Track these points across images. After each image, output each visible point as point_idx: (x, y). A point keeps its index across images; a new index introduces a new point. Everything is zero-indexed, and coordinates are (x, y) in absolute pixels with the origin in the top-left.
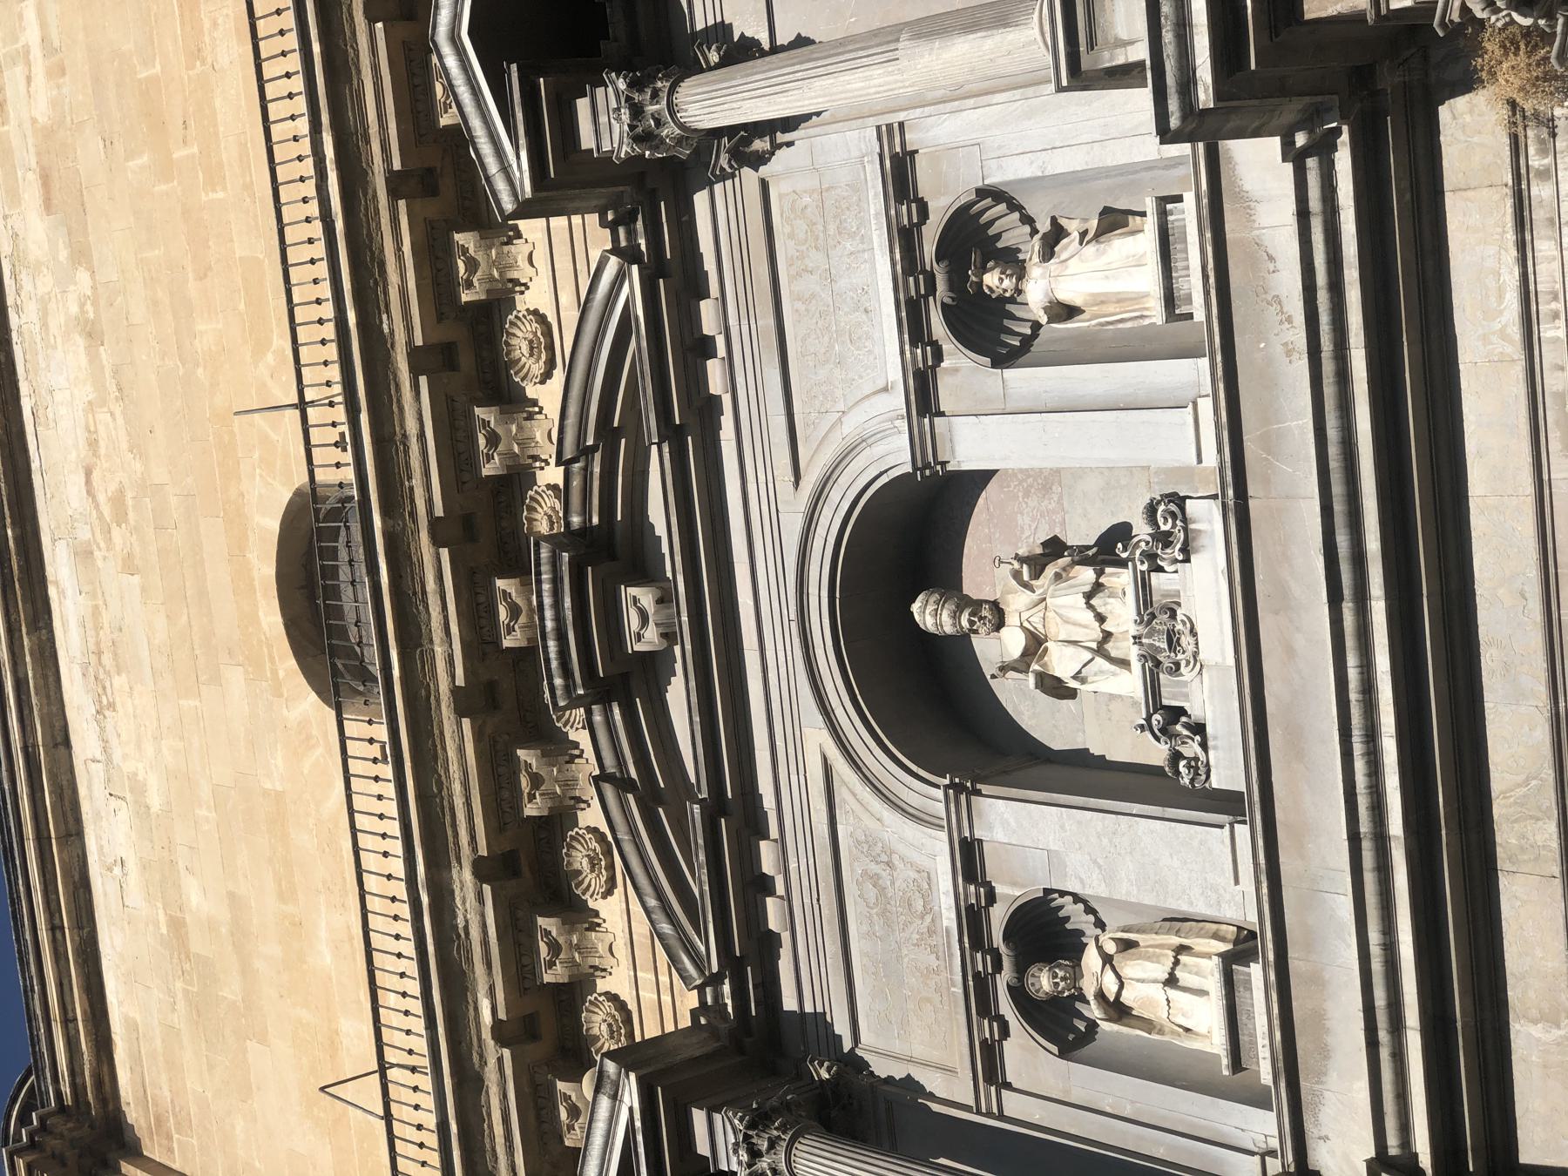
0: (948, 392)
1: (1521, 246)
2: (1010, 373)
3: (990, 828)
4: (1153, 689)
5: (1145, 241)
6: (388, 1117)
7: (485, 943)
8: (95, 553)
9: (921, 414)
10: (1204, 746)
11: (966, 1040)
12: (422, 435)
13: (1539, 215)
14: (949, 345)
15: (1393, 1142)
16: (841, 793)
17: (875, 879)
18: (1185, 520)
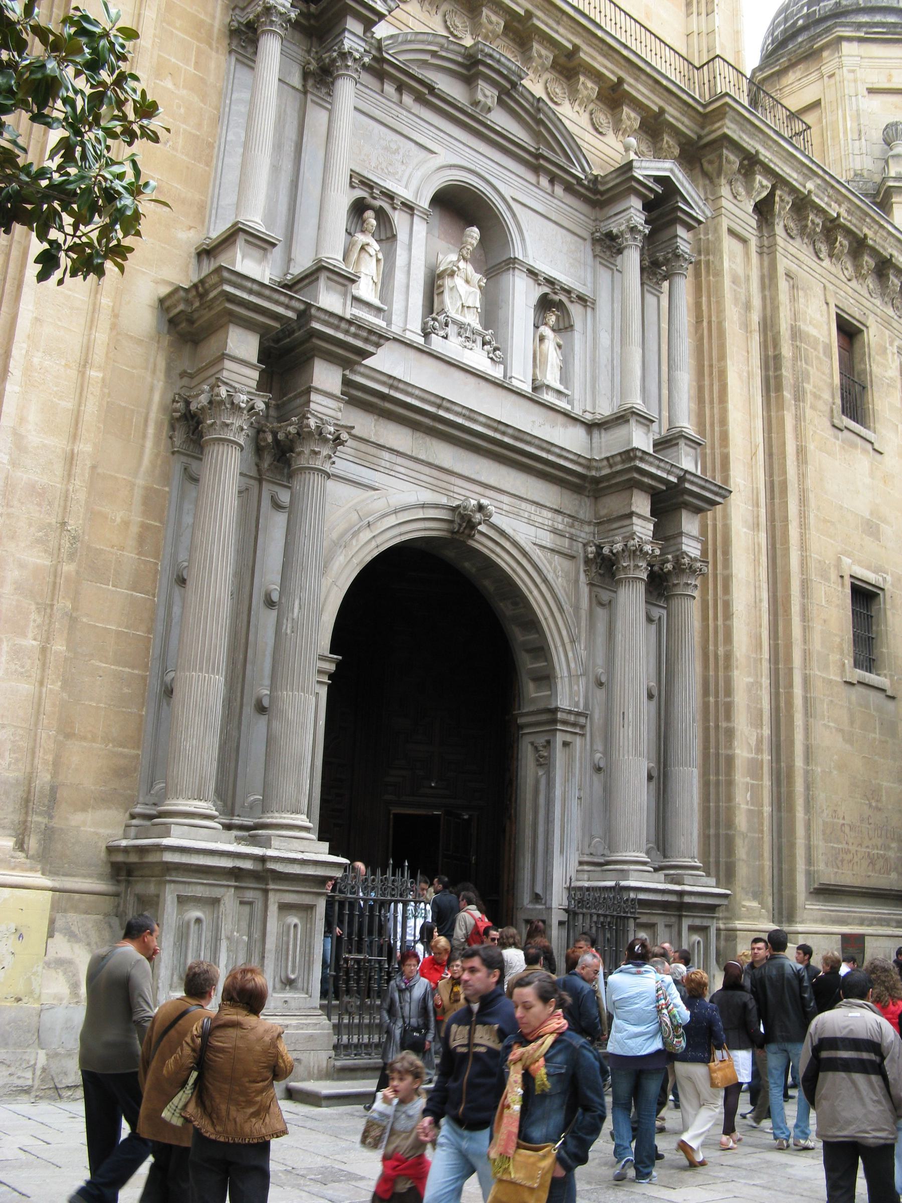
1: (552, 509)
9: (528, 270)
12: (557, 32)
16: (424, 154)
17: (397, 151)
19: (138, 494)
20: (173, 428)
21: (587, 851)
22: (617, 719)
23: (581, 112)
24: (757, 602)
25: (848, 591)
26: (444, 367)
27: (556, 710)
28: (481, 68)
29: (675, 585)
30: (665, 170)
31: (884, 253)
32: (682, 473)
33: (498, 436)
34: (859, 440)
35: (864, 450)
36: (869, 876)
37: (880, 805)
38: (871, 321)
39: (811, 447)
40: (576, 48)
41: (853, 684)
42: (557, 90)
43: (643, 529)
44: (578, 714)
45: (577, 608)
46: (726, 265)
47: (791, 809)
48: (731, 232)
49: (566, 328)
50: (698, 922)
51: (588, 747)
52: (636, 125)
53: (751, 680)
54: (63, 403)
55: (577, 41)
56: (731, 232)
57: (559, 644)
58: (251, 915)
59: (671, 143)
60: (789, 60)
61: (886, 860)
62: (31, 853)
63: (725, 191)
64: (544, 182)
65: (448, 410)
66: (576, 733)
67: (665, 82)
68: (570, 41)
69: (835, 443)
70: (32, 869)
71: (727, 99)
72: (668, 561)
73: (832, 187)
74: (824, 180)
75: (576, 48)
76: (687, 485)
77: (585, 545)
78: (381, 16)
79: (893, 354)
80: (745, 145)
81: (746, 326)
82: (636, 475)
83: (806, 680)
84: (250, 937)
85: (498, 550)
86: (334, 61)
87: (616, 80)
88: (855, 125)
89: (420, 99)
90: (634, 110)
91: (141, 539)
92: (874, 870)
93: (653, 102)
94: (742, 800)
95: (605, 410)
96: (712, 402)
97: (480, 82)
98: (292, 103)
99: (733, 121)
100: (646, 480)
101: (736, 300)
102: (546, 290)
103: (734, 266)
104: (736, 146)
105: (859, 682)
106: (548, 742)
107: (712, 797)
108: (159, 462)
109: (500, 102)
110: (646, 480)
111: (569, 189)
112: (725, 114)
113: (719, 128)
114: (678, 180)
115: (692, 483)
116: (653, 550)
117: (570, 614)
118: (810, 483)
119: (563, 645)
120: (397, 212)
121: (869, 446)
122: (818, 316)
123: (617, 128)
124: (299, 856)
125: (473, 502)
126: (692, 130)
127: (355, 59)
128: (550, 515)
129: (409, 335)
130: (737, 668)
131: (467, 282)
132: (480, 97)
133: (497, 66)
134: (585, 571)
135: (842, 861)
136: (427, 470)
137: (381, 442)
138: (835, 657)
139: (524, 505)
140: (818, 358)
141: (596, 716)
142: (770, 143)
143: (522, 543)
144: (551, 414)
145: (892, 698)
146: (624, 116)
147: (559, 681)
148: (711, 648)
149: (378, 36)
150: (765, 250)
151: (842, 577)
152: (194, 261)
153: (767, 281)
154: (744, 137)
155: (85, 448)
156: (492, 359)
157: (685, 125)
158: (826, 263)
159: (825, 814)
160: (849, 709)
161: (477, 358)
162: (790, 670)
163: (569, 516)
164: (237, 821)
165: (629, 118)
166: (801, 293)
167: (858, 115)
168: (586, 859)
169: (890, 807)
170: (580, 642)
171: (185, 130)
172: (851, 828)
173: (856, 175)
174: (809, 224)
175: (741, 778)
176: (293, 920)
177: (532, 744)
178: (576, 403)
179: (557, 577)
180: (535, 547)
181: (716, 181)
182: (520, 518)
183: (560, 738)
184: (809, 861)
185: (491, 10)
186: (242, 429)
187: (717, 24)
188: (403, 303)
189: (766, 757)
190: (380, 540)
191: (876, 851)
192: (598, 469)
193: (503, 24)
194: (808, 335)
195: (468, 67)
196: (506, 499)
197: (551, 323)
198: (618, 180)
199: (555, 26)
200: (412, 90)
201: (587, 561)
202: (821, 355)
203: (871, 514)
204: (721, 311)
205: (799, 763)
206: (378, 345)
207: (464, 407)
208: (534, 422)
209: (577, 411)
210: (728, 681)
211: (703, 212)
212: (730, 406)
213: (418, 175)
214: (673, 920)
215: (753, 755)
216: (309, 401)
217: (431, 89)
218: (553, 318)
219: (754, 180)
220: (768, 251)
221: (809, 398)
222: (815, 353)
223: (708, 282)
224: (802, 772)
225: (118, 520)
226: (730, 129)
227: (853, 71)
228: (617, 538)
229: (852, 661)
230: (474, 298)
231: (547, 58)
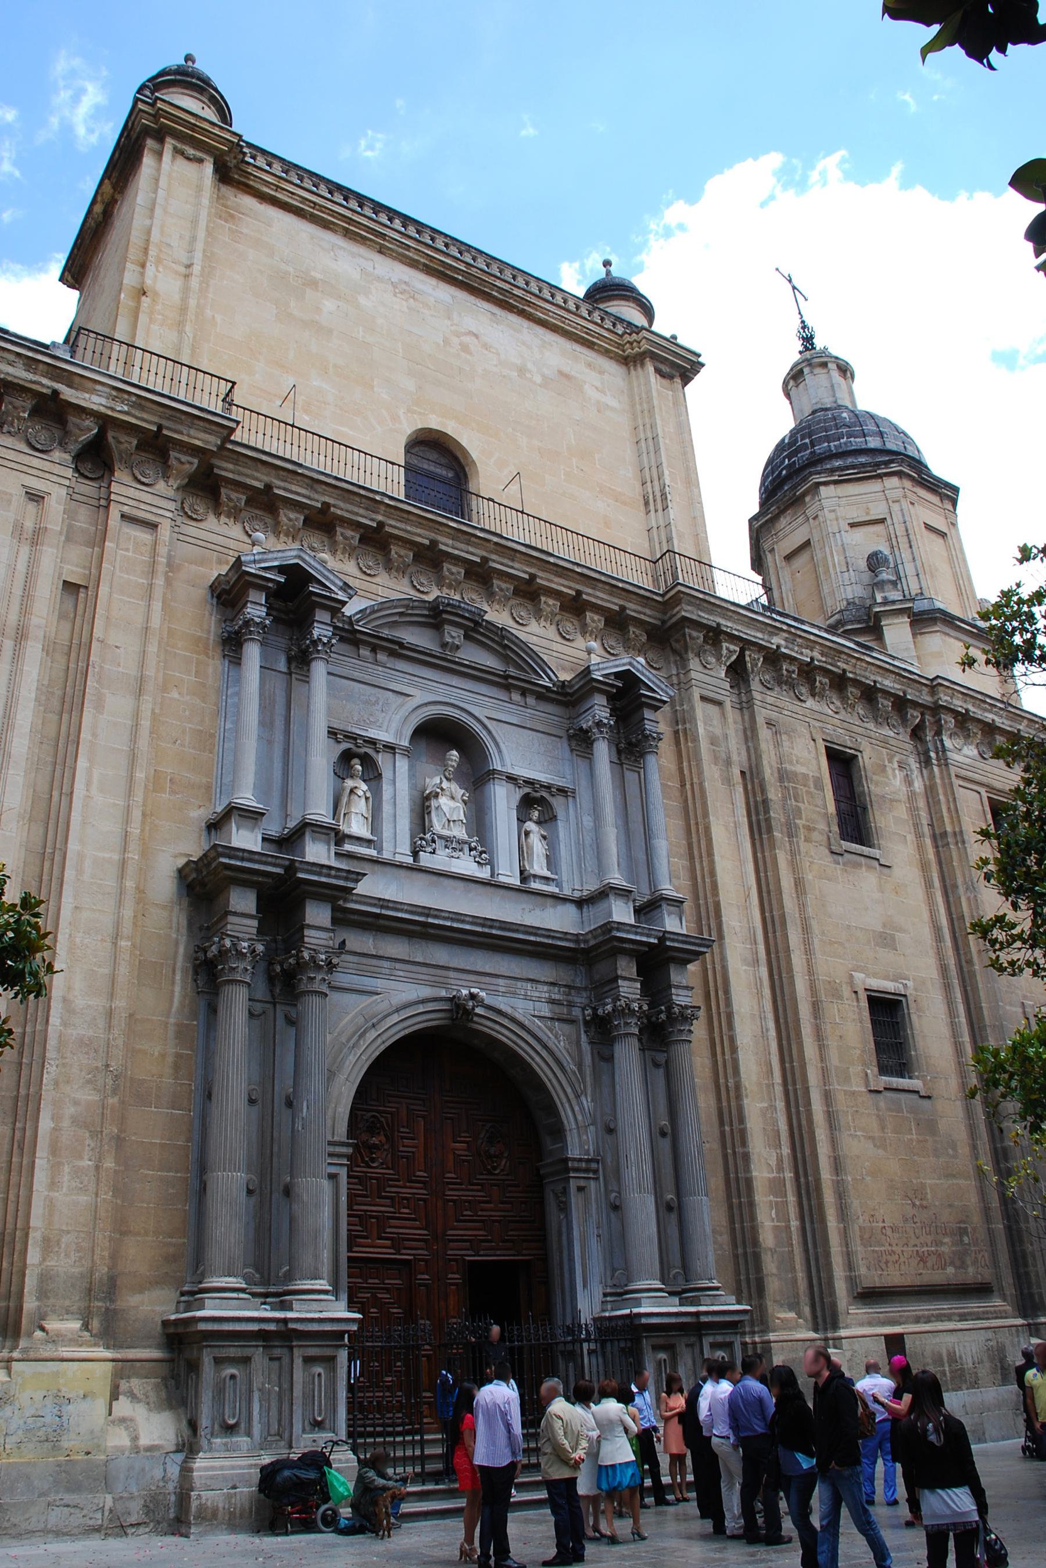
5: (546, 873)
6: (293, 426)
8: (449, 323)
12: (512, 567)
17: (377, 702)
20: (196, 973)
21: (609, 1282)
22: (622, 1161)
23: (548, 625)
24: (764, 1032)
25: (864, 1004)
26: (434, 878)
27: (566, 1160)
28: (444, 616)
29: (671, 1032)
30: (624, 665)
31: (867, 682)
32: (661, 934)
33: (486, 930)
34: (862, 859)
35: (870, 868)
36: (921, 1274)
37: (924, 1203)
38: (864, 745)
39: (809, 877)
40: (533, 577)
41: (880, 1092)
42: (522, 613)
43: (630, 990)
44: (588, 1161)
45: (580, 1065)
46: (701, 731)
47: (823, 1220)
48: (704, 698)
50: (720, 1339)
51: (602, 1189)
52: (601, 625)
53: (766, 1105)
54: (101, 970)
55: (532, 571)
56: (704, 698)
57: (564, 1100)
58: (281, 1367)
59: (638, 632)
60: (778, 508)
61: (939, 1256)
62: (94, 1332)
63: (694, 664)
64: (516, 697)
65: (436, 917)
66: (589, 1178)
67: (620, 585)
69: (835, 869)
70: (96, 1345)
71: (680, 588)
72: (661, 1012)
73: (800, 637)
74: (790, 633)
75: (533, 577)
76: (668, 943)
77: (583, 1009)
78: (344, 603)
79: (894, 770)
80: (705, 621)
81: (728, 781)
82: (616, 944)
83: (828, 1097)
84: (280, 1388)
85: (497, 1027)
86: (308, 646)
87: (574, 593)
88: (842, 558)
89: (392, 654)
90: (597, 613)
91: (176, 1067)
92: (925, 1267)
94: (766, 1219)
95: (592, 886)
96: (701, 857)
97: (446, 627)
98: (278, 684)
99: (689, 604)
100: (626, 946)
101: (716, 759)
102: (527, 790)
103: (711, 729)
104: (697, 625)
105: (885, 1089)
106: (565, 1188)
107: (737, 1218)
108: (187, 1002)
109: (467, 637)
110: (626, 946)
112: (681, 599)
114: (638, 670)
115: (673, 940)
116: (640, 1008)
117: (574, 1073)
118: (810, 911)
119: (569, 1101)
120: (380, 755)
121: (876, 863)
122: (806, 754)
123: (584, 631)
124: (317, 1315)
125: (465, 992)
126: (655, 618)
127: (324, 644)
128: (546, 988)
129: (399, 858)
130: (747, 1096)
131: (453, 798)
132: (449, 640)
134: (585, 1032)
135: (887, 1262)
136: (424, 970)
137: (381, 953)
138: (856, 1070)
139: (519, 984)
140: (808, 793)
141: (609, 1160)
142: (730, 614)
143: (521, 1018)
144: (539, 898)
145: (929, 1097)
146: (588, 620)
147: (568, 1133)
148: (722, 1081)
149: (348, 614)
150: (744, 705)
151: (856, 992)
152: (204, 833)
153: (749, 733)
154: (703, 614)
155: (120, 1003)
156: (478, 862)
157: (648, 615)
158: (810, 703)
159: (861, 1220)
160: (878, 1116)
161: (465, 865)
162: (807, 1090)
163: (565, 986)
164: (272, 1289)
165: (593, 621)
166: (784, 737)
167: (844, 549)
168: (608, 1290)
169: (937, 1203)
172: (893, 1229)
173: (849, 604)
174: (785, 672)
175: (762, 1198)
176: (318, 1369)
177: (553, 1191)
178: (565, 885)
179: (559, 1042)
181: (685, 656)
183: (573, 1185)
184: (850, 1266)
185: (451, 563)
186: (247, 970)
187: (672, 517)
188: (392, 831)
189: (789, 1175)
190: (384, 1037)
191: (925, 1249)
192: (586, 941)
193: (463, 571)
194: (795, 774)
195: (434, 617)
196: (501, 982)
198: (581, 683)
199: (510, 564)
200: (384, 649)
201: (586, 1023)
202: (812, 790)
203: (884, 926)
204: (700, 773)
205: (826, 1175)
206: (357, 881)
209: (567, 892)
210: (740, 1109)
211: (667, 693)
212: (717, 858)
213: (397, 718)
214: (693, 1339)
215: (775, 1174)
216: (303, 936)
217: (401, 645)
218: (536, 813)
219: (722, 647)
220: (746, 706)
221: (802, 833)
222: (805, 789)
223: (688, 748)
224: (829, 1183)
225: (156, 1054)
226: (687, 611)
227: (834, 511)
228: (609, 1000)
229: (876, 1069)
231: (508, 589)
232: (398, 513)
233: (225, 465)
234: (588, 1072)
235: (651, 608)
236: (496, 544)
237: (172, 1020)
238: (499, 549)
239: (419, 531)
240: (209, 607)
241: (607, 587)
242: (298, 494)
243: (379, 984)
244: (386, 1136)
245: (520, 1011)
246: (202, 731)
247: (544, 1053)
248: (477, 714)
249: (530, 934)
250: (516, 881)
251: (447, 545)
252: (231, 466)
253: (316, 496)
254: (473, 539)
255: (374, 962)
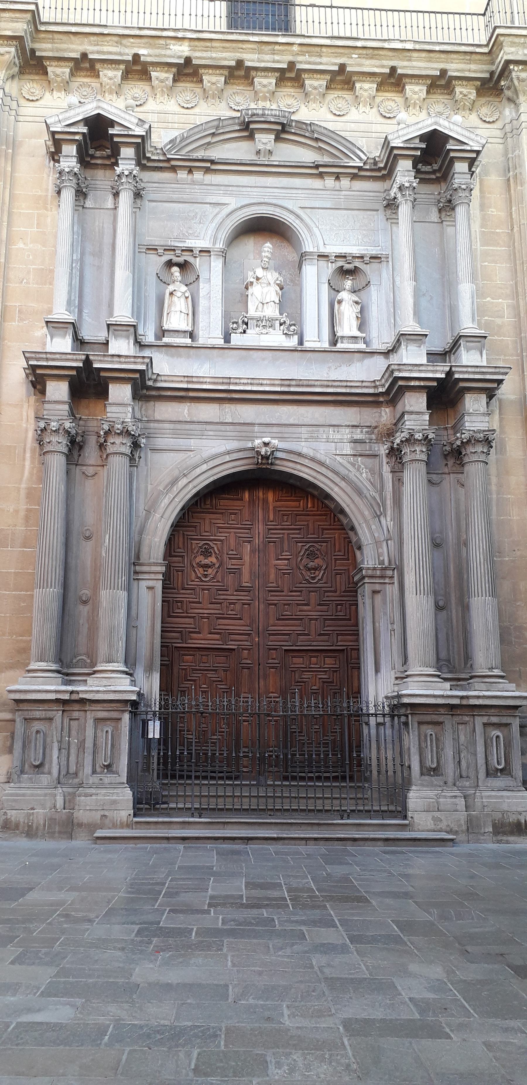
0: (323, 263)
1: (349, 426)
2: (327, 284)
3: (214, 262)
4: (252, 319)
7: (165, 55)
10: (241, 333)
11: (156, 244)
12: (321, 63)
13: (354, 430)
14: (335, 266)
15: (163, 378)
18: (292, 335)
19: (23, 493)
33: (286, 389)
44: (383, 569)
49: (367, 285)
64: (330, 182)
68: (335, 64)
85: (299, 467)
91: (27, 518)
93: (432, 69)
102: (340, 263)
108: (35, 472)
111: (354, 177)
112: (502, 44)
113: (502, 58)
117: (374, 498)
120: (198, 259)
126: (482, 72)
128: (348, 430)
133: (262, 119)
134: (388, 463)
137: (195, 419)
139: (321, 429)
170: (385, 516)
171: (33, 269)
180: (338, 458)
181: (517, 102)
182: (319, 440)
183: (368, 589)
190: (195, 483)
192: (383, 386)
196: (304, 429)
197: (347, 287)
199: (318, 60)
207: (248, 378)
208: (329, 368)
217: (212, 162)
225: (11, 510)
230: (272, 294)
232: (202, 43)
233: (44, 46)
234: (388, 497)
235: (475, 62)
236: (300, 45)
237: (23, 486)
238: (304, 49)
239: (224, 55)
240: (47, 170)
241: (424, 55)
242: (110, 53)
243: (193, 443)
244: (217, 558)
245: (322, 452)
246: (43, 269)
247: (343, 484)
248: (290, 207)
249: (328, 386)
250: (326, 345)
251: (253, 61)
252: (49, 46)
253: (127, 51)
254: (277, 47)
255: (188, 426)
